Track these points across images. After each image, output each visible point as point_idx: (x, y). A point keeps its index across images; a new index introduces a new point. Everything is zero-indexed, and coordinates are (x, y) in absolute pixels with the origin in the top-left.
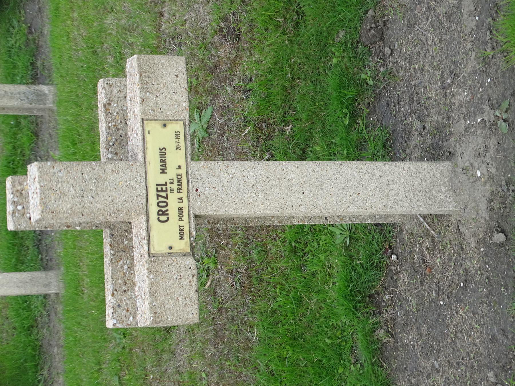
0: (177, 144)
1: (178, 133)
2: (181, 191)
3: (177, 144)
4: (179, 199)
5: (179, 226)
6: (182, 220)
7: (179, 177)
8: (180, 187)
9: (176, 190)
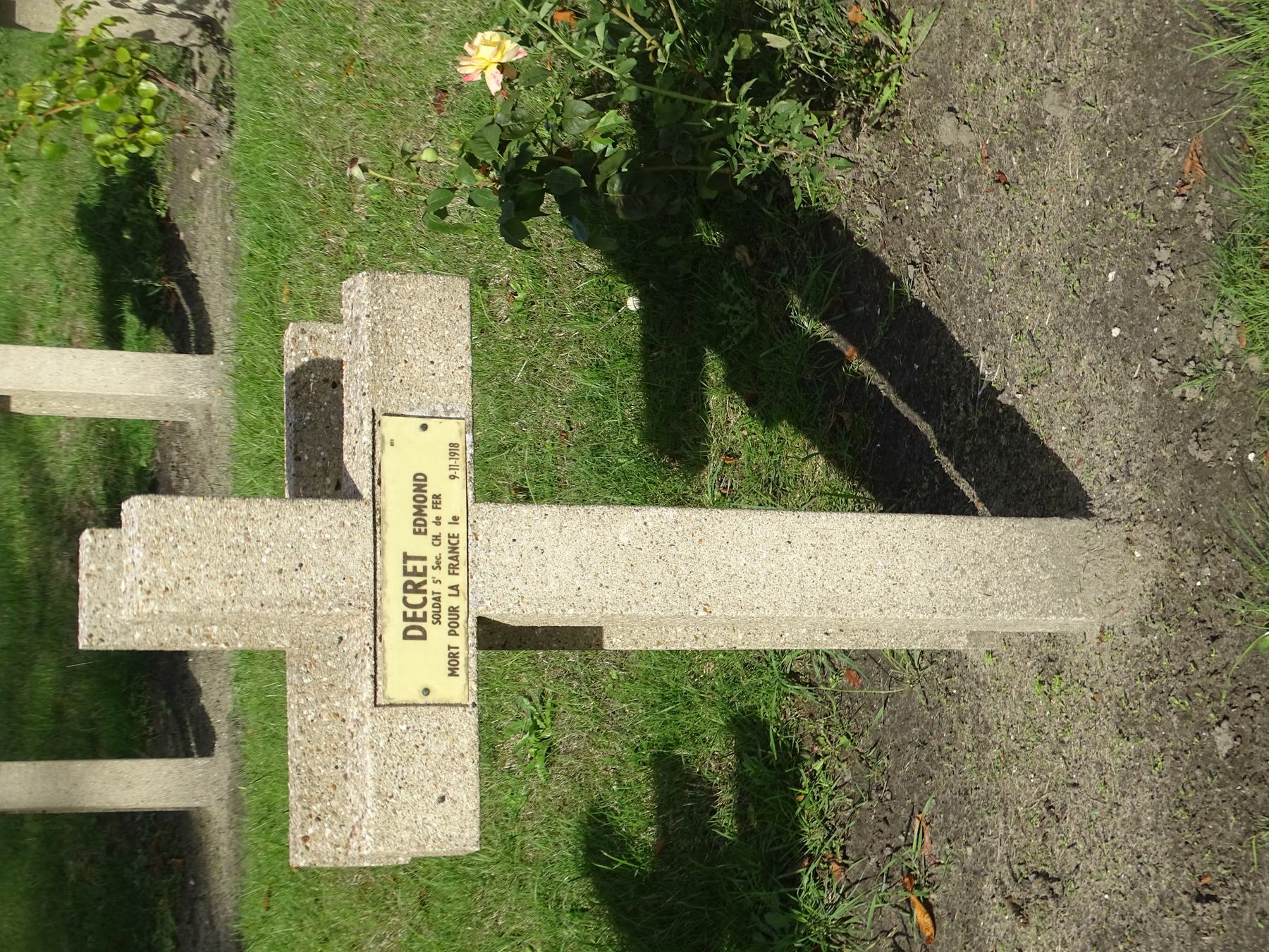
4: (451, 588)
5: (449, 648)
6: (456, 634)
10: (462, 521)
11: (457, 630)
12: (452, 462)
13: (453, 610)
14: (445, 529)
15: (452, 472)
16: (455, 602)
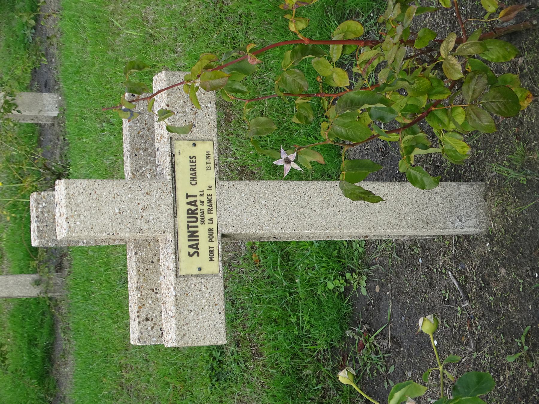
0: (208, 165)
4: (209, 220)
5: (209, 248)
6: (212, 241)
7: (210, 197)
8: (211, 208)
10: (213, 187)
11: (213, 240)
14: (206, 192)
15: (208, 165)
16: (211, 226)
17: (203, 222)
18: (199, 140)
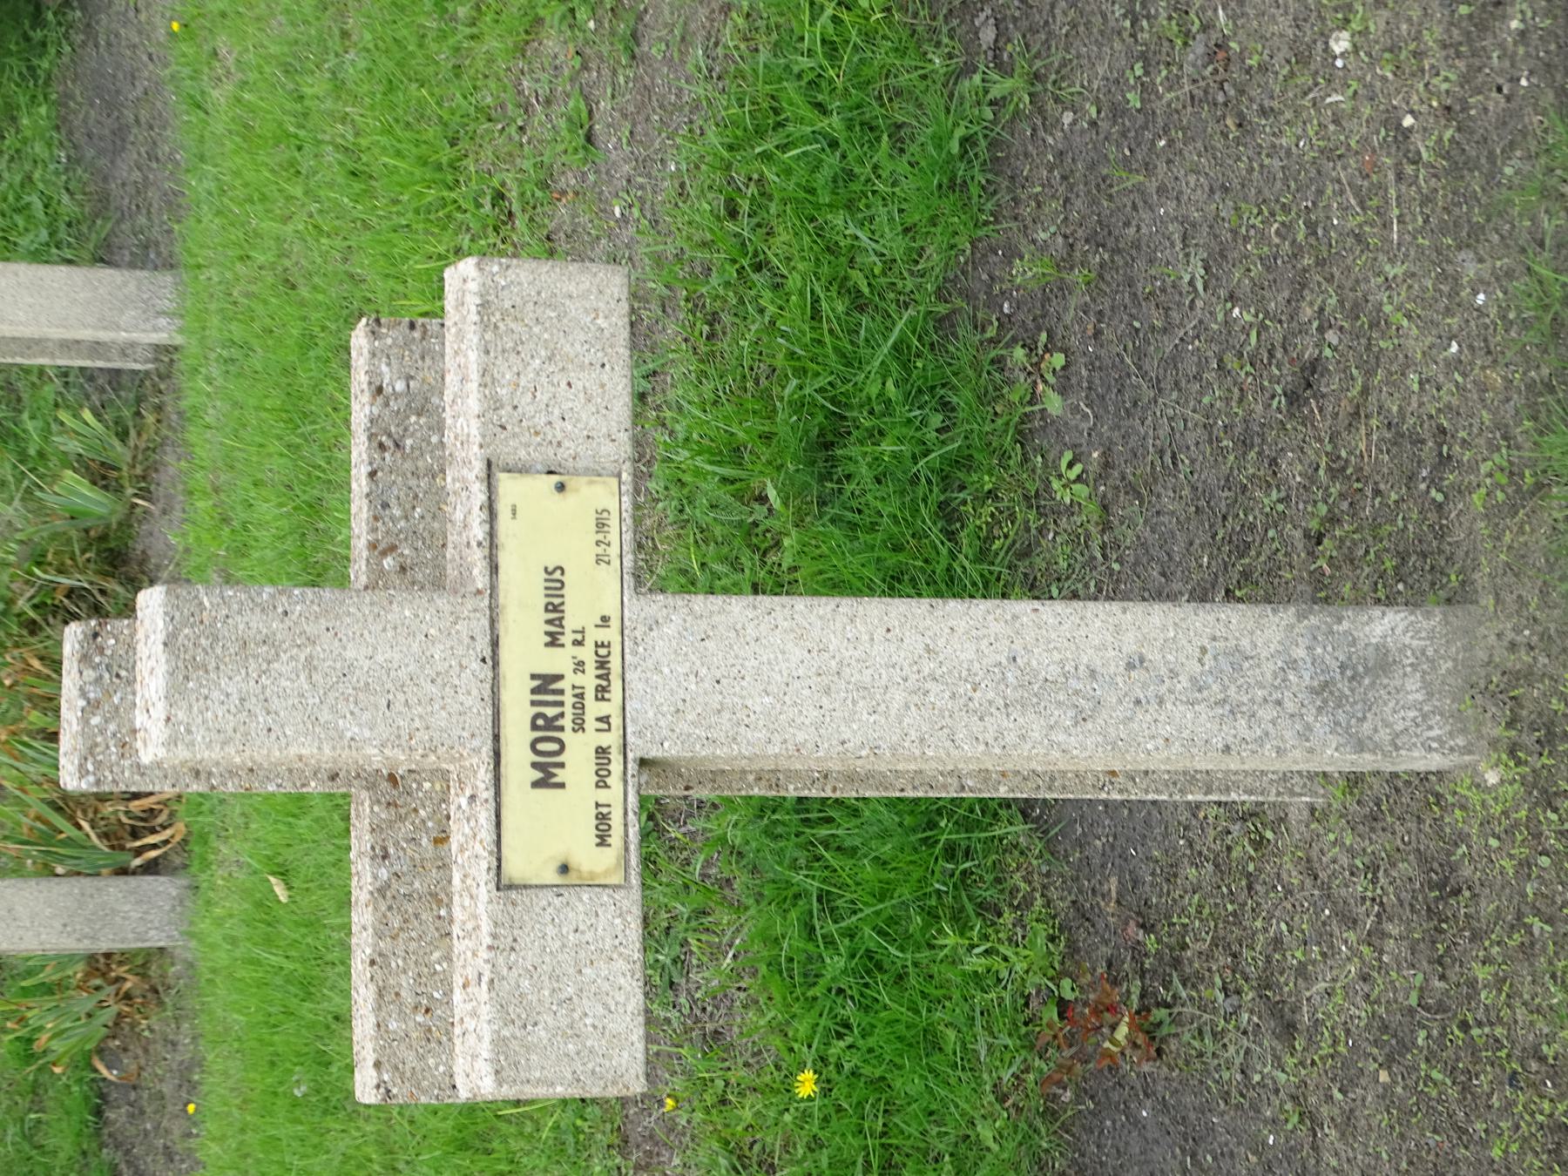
0: (600, 550)
1: (605, 515)
2: (607, 696)
3: (600, 550)
4: (599, 719)
6: (607, 786)
8: (604, 683)
9: (590, 695)
10: (615, 623)
11: (608, 780)
12: (600, 537)
13: (602, 752)
17: (579, 726)
18: (576, 473)
